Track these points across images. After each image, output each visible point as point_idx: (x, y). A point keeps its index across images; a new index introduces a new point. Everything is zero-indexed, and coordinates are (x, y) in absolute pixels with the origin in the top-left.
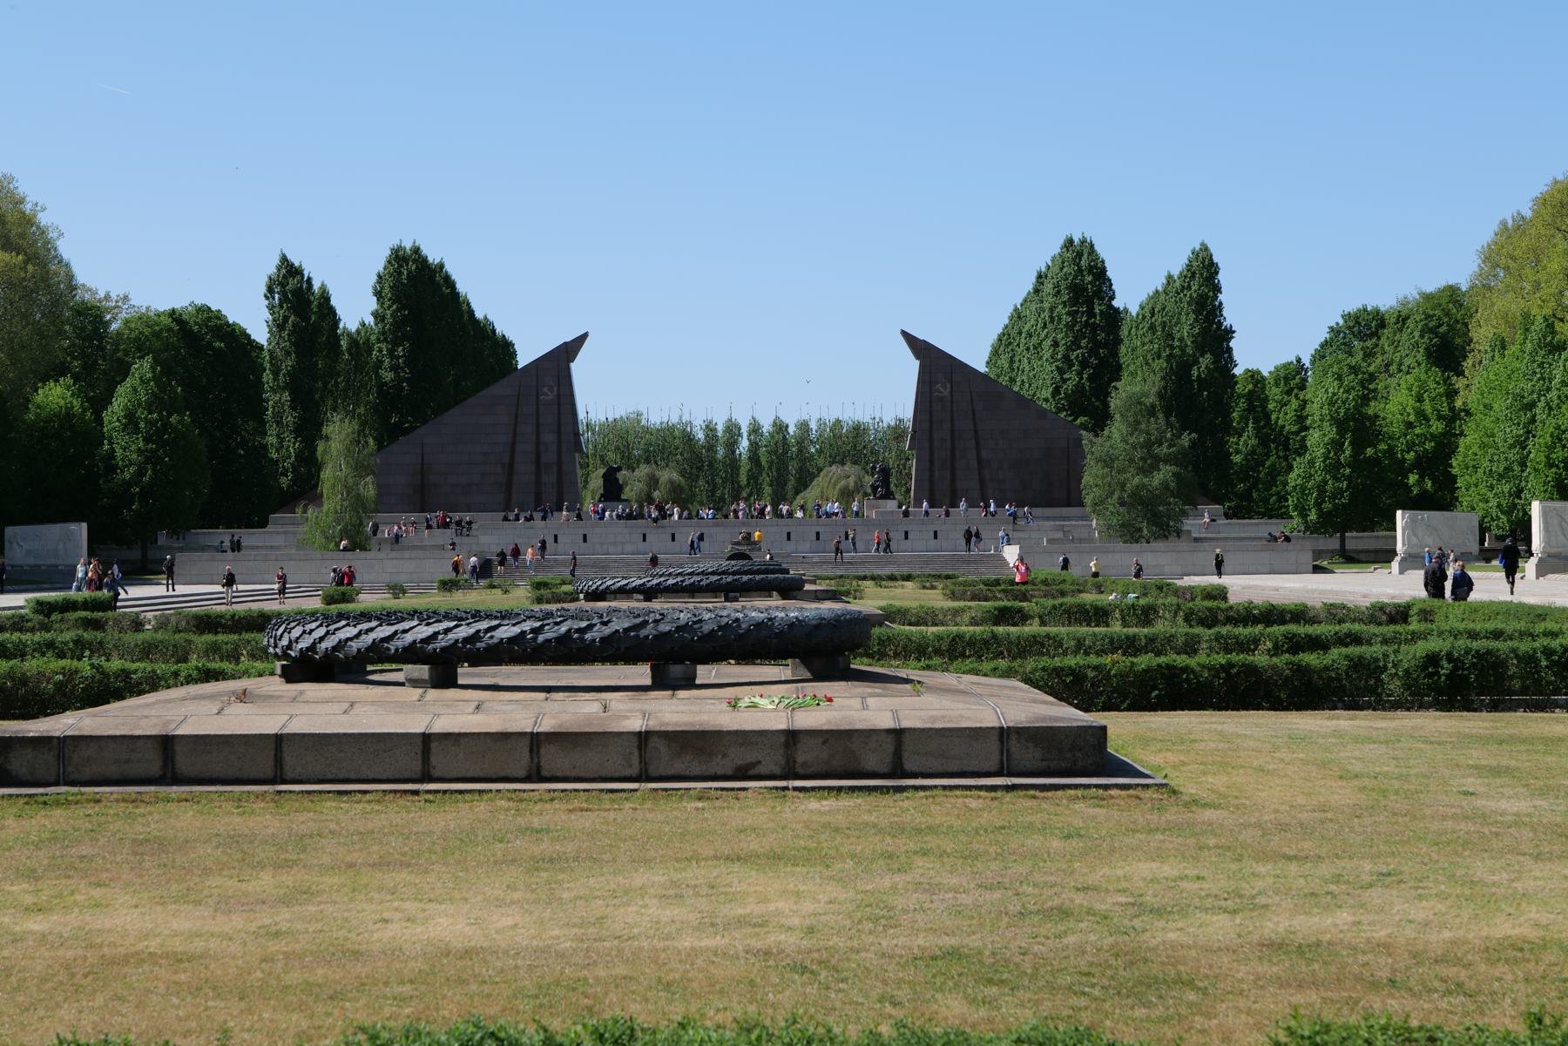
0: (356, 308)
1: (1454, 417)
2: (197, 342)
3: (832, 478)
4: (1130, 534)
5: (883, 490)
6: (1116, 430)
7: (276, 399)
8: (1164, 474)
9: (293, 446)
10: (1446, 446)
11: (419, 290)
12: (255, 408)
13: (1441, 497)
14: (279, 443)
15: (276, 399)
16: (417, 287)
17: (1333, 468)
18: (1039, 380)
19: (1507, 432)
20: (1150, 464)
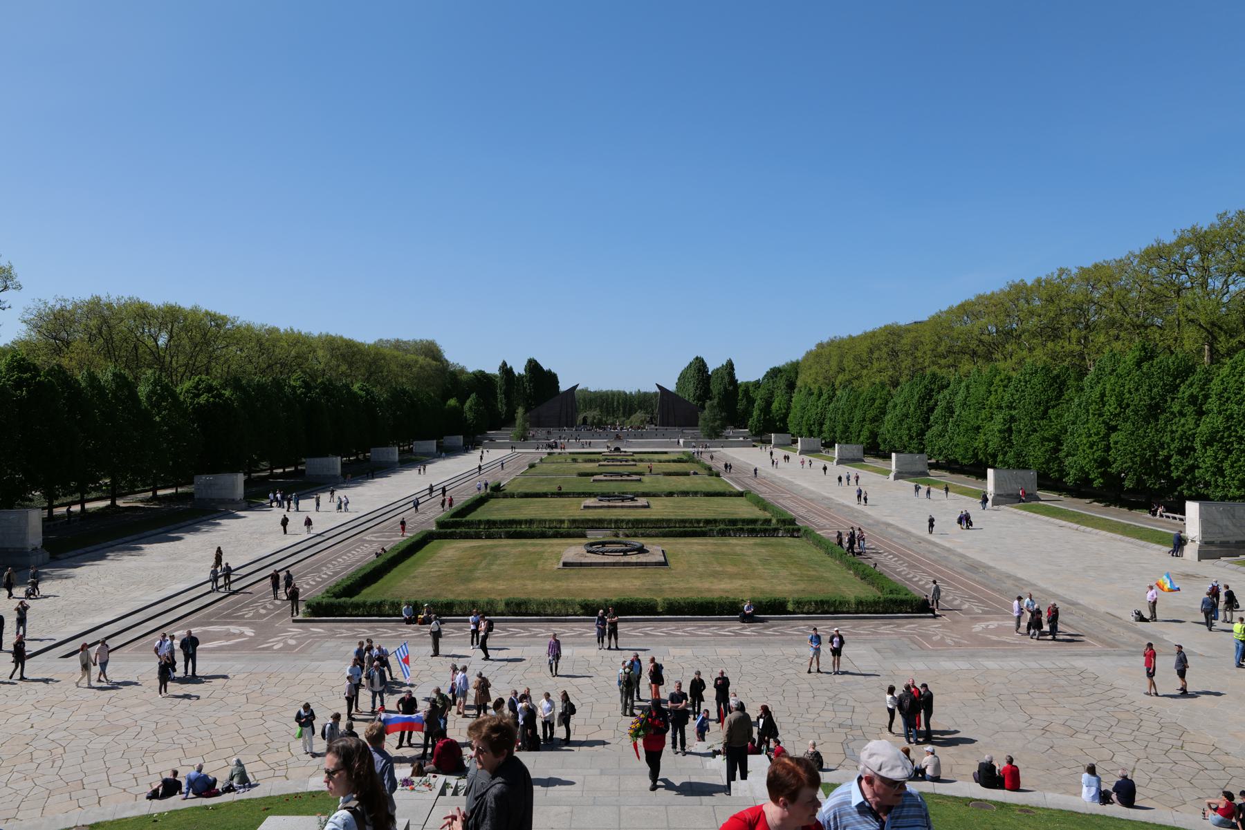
0: (519, 369)
1: (788, 408)
2: (482, 380)
3: (639, 416)
4: (710, 437)
5: (651, 422)
6: (706, 412)
7: (500, 396)
8: (718, 423)
9: (505, 408)
10: (786, 415)
11: (533, 366)
12: (496, 398)
13: (784, 430)
14: (501, 407)
15: (500, 396)
16: (533, 366)
17: (759, 421)
18: (689, 395)
19: (799, 414)
20: (714, 420)
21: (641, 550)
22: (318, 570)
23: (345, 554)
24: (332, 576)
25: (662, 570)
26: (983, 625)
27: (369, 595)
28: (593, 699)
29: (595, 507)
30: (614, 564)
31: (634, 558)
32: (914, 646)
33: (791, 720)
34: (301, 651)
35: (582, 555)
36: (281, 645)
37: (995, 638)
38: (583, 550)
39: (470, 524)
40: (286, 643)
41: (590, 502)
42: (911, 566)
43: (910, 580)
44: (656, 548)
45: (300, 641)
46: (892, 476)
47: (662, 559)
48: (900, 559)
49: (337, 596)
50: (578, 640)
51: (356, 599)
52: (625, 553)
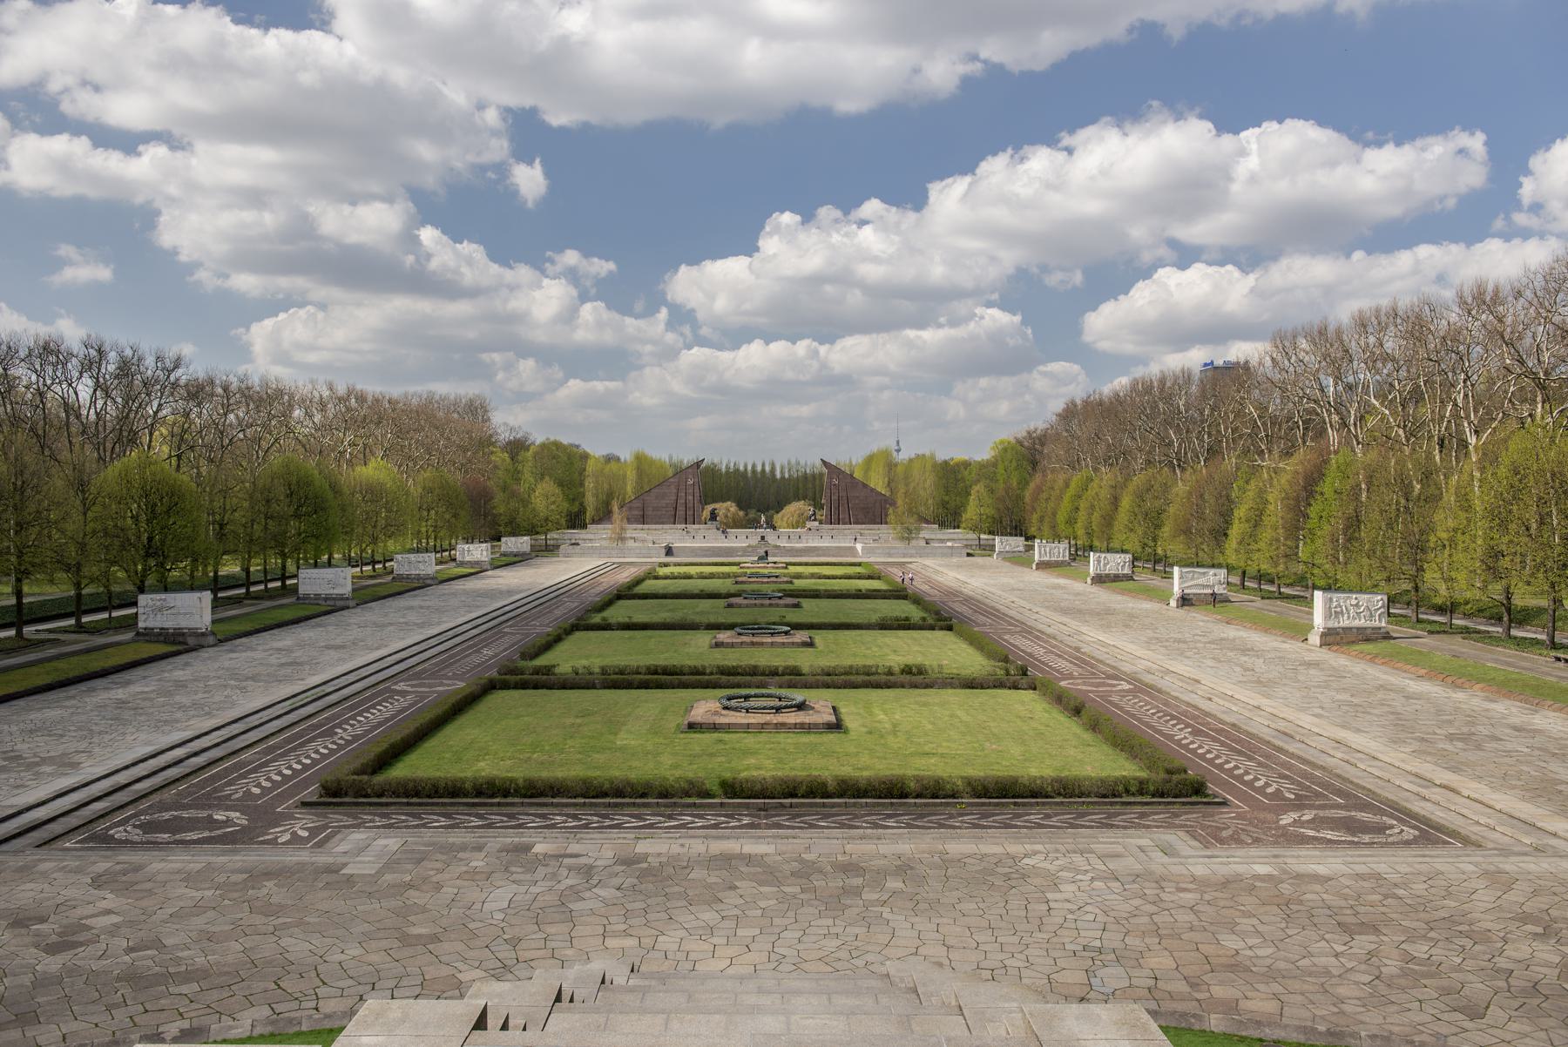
21: (801, 707)
22: (330, 733)
23: (367, 710)
24: (348, 743)
25: (832, 737)
26: (1295, 815)
27: (401, 771)
28: (736, 912)
29: (732, 645)
30: (763, 726)
31: (792, 718)
32: (1196, 844)
33: (1016, 939)
34: (320, 844)
35: (716, 713)
36: (287, 837)
37: (1311, 833)
38: (714, 705)
39: (548, 670)
40: (294, 834)
41: (724, 636)
42: (1196, 733)
43: (1194, 752)
44: (822, 704)
45: (314, 832)
46: (1173, 603)
47: (832, 719)
48: (1180, 721)
49: (355, 773)
50: (713, 831)
51: (379, 779)
52: (778, 710)
